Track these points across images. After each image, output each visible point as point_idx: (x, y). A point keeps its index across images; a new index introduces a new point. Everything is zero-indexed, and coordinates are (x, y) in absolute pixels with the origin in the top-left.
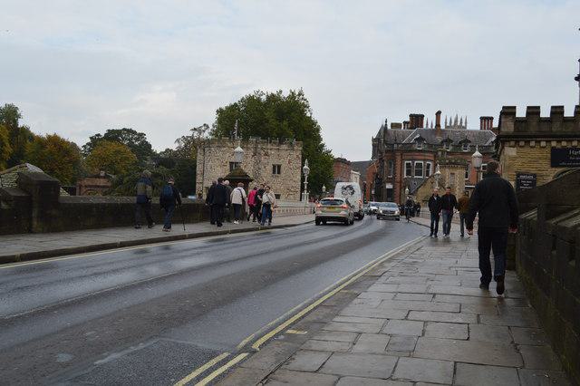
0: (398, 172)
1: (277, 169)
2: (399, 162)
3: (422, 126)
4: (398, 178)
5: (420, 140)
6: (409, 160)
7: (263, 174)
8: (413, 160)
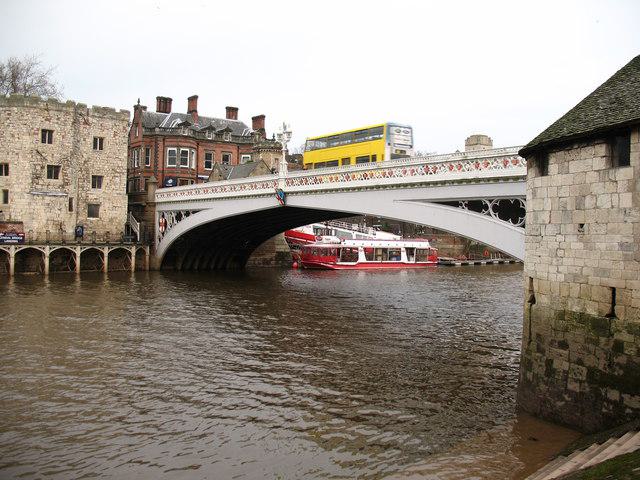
0: (160, 160)
1: (98, 143)
2: (160, 148)
6: (172, 146)
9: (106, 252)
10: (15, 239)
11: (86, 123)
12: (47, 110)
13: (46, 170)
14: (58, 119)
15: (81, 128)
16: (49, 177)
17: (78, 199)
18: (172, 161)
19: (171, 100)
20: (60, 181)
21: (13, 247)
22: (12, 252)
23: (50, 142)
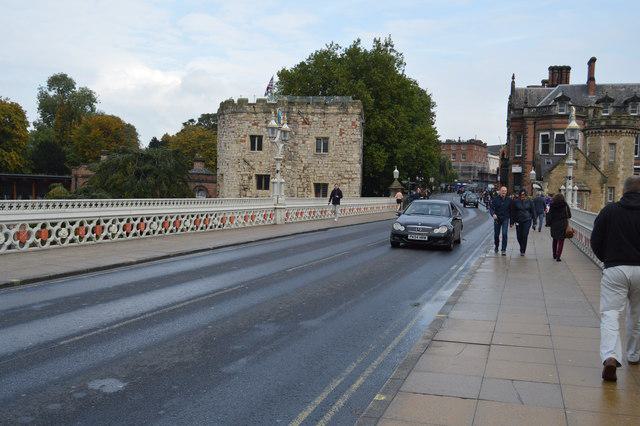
0: (530, 148)
1: (323, 145)
3: (567, 82)
4: (529, 158)
5: (563, 100)
7: (302, 153)
8: (552, 130)
11: (305, 122)
12: (255, 113)
13: (254, 180)
15: (300, 129)
16: (259, 187)
18: (546, 149)
19: (568, 68)
23: (260, 148)
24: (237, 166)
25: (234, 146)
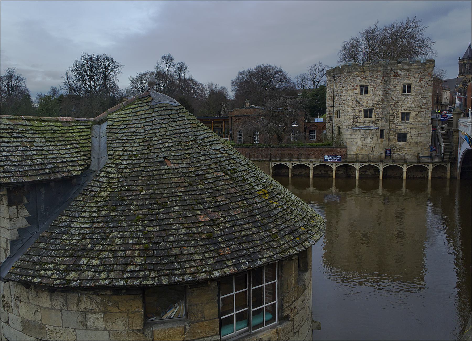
1: (407, 89)
9: (405, 168)
10: (335, 159)
11: (397, 75)
12: (364, 72)
13: (363, 112)
14: (371, 77)
15: (392, 80)
16: (366, 116)
17: (390, 130)
20: (373, 119)
21: (334, 164)
22: (334, 167)
23: (366, 93)
24: (351, 104)
25: (349, 92)
